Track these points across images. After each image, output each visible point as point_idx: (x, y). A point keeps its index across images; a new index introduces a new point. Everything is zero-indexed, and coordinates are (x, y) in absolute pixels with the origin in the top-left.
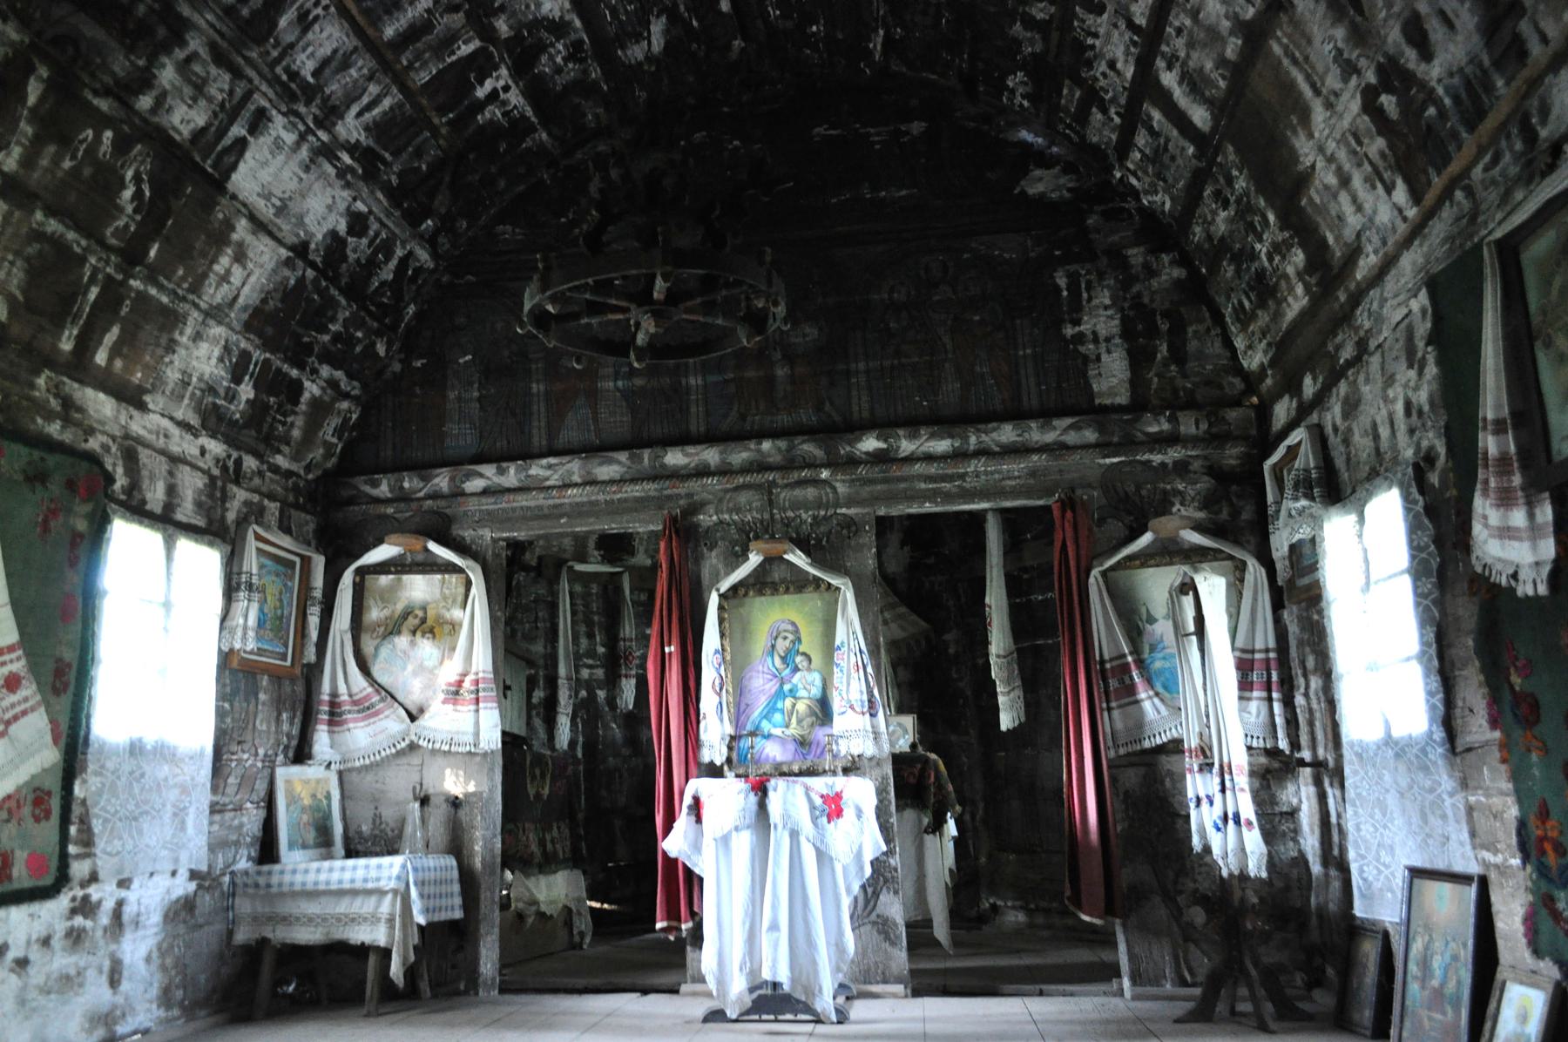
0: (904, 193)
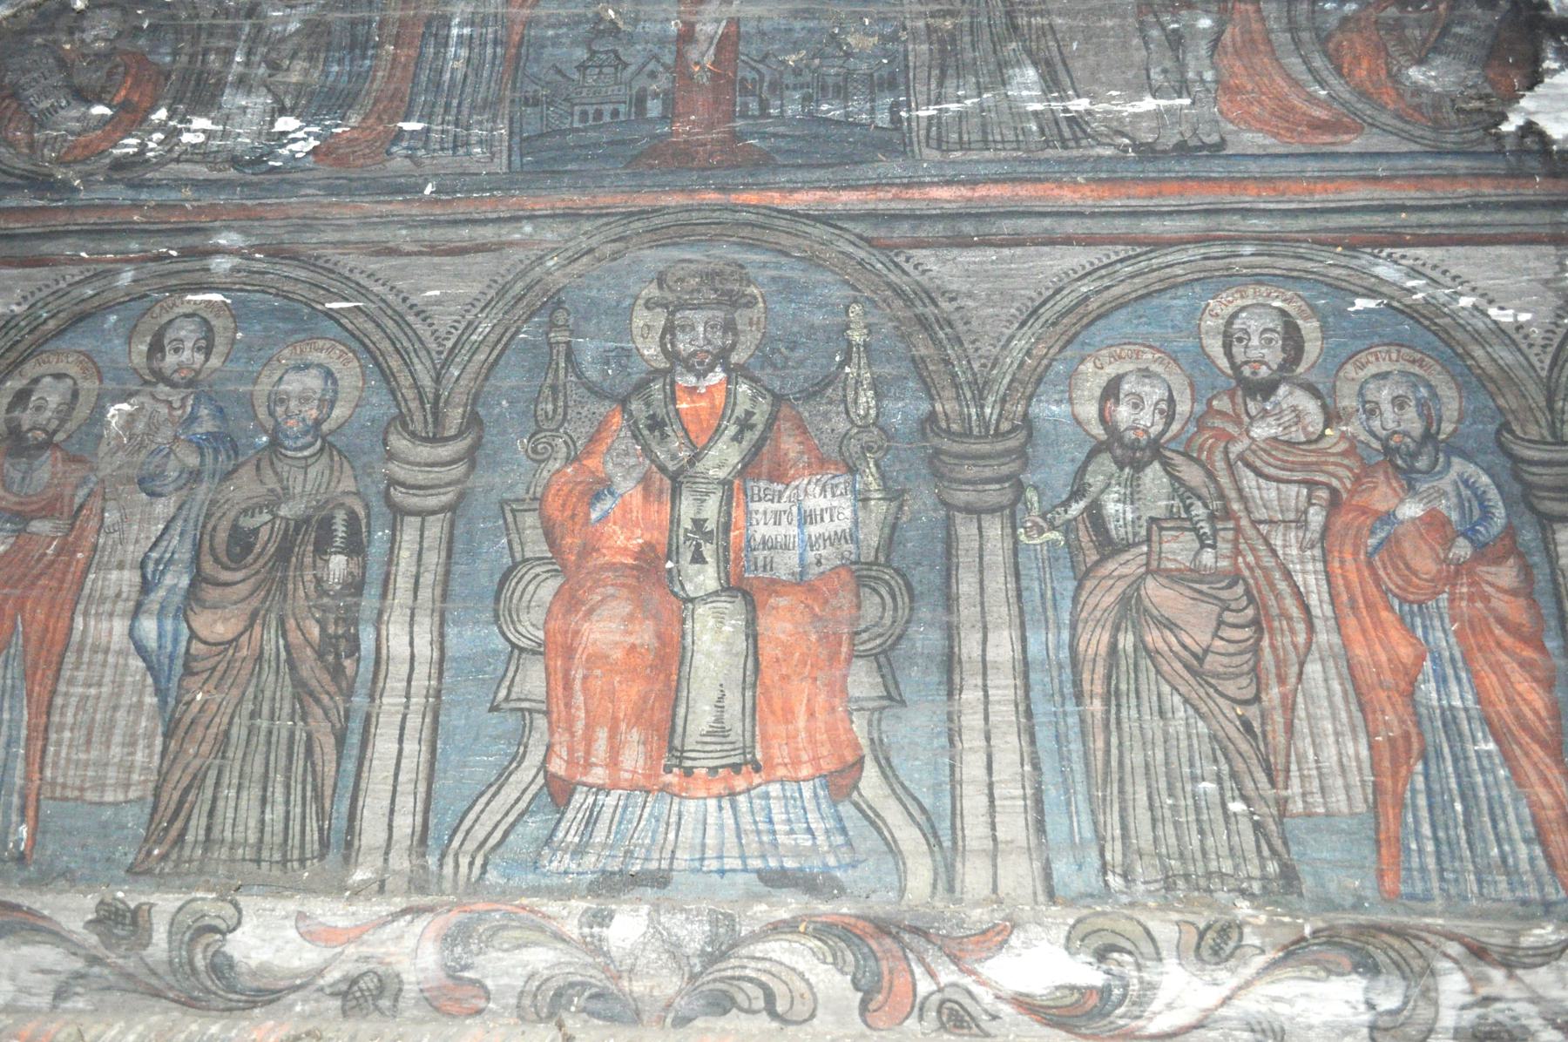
0: (1148, 104)
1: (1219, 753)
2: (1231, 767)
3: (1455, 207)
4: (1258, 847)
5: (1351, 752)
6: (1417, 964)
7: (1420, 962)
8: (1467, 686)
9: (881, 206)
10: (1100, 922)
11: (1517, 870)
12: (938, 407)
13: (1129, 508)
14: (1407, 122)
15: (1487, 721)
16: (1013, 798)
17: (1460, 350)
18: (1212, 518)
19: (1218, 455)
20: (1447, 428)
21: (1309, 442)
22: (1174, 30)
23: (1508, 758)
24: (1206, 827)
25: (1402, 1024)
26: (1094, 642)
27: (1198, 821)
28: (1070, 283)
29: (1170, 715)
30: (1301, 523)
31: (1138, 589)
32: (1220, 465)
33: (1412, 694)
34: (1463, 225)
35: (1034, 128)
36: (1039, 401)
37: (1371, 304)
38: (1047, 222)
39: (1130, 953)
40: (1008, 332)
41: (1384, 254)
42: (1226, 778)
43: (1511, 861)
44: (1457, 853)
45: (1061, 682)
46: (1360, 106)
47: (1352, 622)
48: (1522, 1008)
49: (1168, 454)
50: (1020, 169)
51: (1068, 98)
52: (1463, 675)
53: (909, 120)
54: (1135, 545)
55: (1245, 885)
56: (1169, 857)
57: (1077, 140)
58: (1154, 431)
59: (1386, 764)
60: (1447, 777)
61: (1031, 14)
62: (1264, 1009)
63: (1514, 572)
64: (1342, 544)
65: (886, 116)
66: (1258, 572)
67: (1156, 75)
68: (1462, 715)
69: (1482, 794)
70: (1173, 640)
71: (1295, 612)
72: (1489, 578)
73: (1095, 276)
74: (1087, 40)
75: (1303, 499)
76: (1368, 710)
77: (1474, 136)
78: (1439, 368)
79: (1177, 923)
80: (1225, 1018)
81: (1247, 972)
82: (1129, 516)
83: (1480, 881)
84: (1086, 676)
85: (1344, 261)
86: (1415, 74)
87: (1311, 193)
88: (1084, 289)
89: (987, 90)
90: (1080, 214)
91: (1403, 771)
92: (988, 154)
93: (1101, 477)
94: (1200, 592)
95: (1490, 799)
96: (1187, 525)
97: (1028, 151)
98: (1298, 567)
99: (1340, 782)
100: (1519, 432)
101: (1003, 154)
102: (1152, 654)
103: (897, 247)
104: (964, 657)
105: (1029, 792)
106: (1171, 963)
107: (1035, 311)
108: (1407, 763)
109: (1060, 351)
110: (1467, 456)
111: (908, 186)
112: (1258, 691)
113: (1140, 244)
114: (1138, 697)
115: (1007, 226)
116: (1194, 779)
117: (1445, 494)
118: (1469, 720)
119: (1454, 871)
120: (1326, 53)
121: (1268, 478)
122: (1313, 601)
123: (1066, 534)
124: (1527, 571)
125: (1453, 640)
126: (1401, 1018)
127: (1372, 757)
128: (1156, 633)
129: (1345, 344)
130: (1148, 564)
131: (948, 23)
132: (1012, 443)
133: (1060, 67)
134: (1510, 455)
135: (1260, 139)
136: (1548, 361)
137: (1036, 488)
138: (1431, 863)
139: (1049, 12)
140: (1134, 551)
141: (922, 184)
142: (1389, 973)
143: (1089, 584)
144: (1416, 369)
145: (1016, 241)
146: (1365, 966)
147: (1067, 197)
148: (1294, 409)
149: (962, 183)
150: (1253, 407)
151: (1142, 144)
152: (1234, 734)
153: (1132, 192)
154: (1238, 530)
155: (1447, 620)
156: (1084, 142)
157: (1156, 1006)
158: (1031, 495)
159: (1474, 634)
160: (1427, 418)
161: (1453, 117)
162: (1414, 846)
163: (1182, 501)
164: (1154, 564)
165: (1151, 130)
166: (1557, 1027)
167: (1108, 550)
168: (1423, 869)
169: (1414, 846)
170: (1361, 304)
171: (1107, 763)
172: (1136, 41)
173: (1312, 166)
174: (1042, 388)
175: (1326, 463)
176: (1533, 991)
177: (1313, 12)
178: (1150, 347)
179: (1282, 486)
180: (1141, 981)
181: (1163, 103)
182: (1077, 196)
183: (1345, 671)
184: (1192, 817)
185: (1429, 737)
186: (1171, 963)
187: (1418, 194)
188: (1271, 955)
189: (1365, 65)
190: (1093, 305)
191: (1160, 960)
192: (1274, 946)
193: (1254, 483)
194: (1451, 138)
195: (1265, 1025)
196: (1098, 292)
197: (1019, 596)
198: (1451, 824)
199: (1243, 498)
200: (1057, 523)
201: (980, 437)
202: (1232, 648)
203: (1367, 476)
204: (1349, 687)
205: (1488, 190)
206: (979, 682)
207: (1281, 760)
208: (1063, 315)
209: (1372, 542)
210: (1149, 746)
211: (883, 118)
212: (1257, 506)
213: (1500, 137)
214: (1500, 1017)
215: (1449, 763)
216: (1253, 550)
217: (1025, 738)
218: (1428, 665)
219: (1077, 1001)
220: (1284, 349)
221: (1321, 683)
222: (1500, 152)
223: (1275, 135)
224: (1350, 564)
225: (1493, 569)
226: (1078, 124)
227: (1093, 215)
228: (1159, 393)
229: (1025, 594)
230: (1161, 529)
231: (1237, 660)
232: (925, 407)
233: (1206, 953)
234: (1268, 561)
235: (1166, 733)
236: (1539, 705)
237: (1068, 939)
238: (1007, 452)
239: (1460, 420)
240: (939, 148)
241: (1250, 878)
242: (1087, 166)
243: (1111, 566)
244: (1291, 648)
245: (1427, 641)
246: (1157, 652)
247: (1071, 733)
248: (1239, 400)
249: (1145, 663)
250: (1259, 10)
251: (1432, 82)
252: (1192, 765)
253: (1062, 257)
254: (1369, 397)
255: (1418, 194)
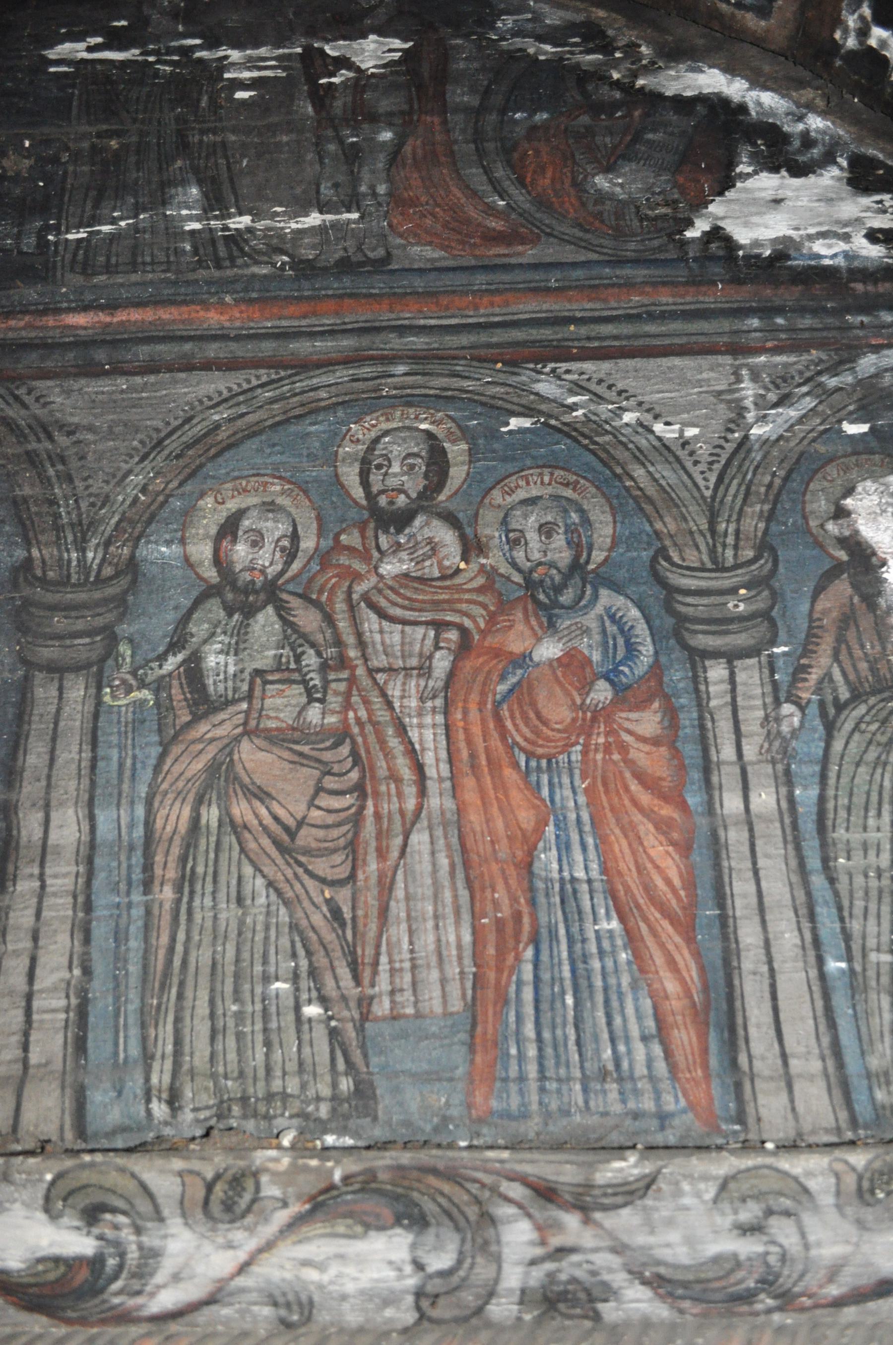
0: (314, 219)
1: (299, 945)
2: (311, 964)
3: (630, 318)
4: (333, 1060)
5: (452, 938)
6: (472, 1212)
7: (476, 1208)
8: (592, 854)
9: (10, 335)
10: (86, 1177)
11: (632, 1078)
12: (35, 553)
13: (231, 660)
14: (587, 231)
15: (612, 893)
16: (54, 1011)
17: (619, 471)
18: (324, 668)
19: (340, 596)
20: (598, 556)
21: (443, 578)
22: (353, 143)
23: (632, 938)
24: (274, 1038)
25: (457, 1288)
26: (173, 818)
27: (265, 1030)
28: (202, 412)
29: (248, 902)
30: (424, 670)
31: (231, 754)
32: (340, 606)
33: (530, 865)
34: (635, 336)
35: (188, 248)
36: (148, 542)
37: (526, 423)
38: (188, 347)
39: (124, 1213)
40: (125, 467)
41: (547, 370)
42: (304, 975)
43: (625, 1065)
44: (563, 1058)
45: (129, 867)
46: (538, 215)
47: (469, 782)
48: (603, 1259)
49: (284, 596)
50: (166, 292)
51: (230, 216)
52: (590, 841)
53: (56, 244)
54: (235, 701)
55: (311, 1108)
56: (226, 1077)
57: (232, 259)
58: (271, 571)
59: (491, 951)
60: (560, 964)
61: (203, 132)
62: (288, 1275)
63: (658, 717)
64: (468, 693)
65: (33, 240)
66: (369, 728)
67: (326, 191)
68: (585, 887)
69: (598, 983)
70: (263, 811)
71: (407, 774)
72: (627, 725)
73: (231, 403)
74: (259, 156)
75: (429, 642)
76: (477, 885)
77: (656, 243)
78: (593, 490)
79: (180, 1174)
80: (243, 1290)
81: (269, 1230)
82: (231, 669)
83: (585, 1090)
84: (159, 858)
85: (501, 378)
86: (601, 182)
87: (476, 307)
88: (216, 417)
89: (145, 210)
90: (224, 338)
91: (510, 959)
92: (135, 278)
93: (206, 626)
94: (301, 754)
95: (606, 989)
96: (296, 676)
97: (178, 272)
98: (415, 721)
99: (435, 975)
100: (676, 559)
101: (150, 276)
102: (237, 829)
103: (20, 379)
104: (24, 840)
105: (74, 1001)
106: (175, 1224)
107: (160, 442)
108: (516, 948)
109: (181, 485)
110: (617, 588)
111: (44, 312)
112: (354, 868)
113: (285, 368)
114: (215, 881)
115: (144, 351)
116: (266, 979)
117: (587, 631)
118: (591, 892)
119: (559, 1080)
120: (509, 164)
121: (393, 620)
122: (429, 758)
123: (157, 692)
124: (671, 714)
125: (582, 799)
126: (455, 1280)
127: (475, 943)
128: (244, 804)
129: (494, 467)
130: (245, 724)
131: (114, 144)
132: (110, 591)
133: (226, 188)
134: (662, 582)
135: (430, 253)
136: (713, 479)
137: (131, 641)
138: (532, 1070)
139: (223, 130)
140: (231, 709)
141: (57, 311)
142: (439, 1224)
143: (176, 750)
144: (568, 493)
145: (151, 368)
146: (410, 1217)
147: (213, 319)
148: (430, 541)
149: (101, 308)
150: (384, 541)
151: (301, 261)
152: (317, 919)
153: (286, 312)
154: (352, 681)
155: (577, 777)
156: (240, 261)
157: (159, 1278)
158: (125, 649)
159: (607, 792)
160: (575, 545)
161: (636, 223)
162: (513, 1051)
163: (293, 649)
164: (253, 723)
165: (314, 247)
166: (645, 1282)
167: (202, 708)
168: (522, 1078)
169: (513, 1051)
170: (515, 423)
171: (169, 962)
172: (310, 156)
173: (480, 280)
174: (153, 526)
175: (460, 601)
176: (616, 1239)
177: (502, 122)
178: (280, 478)
179: (408, 629)
180: (141, 1247)
181: (329, 217)
182: (227, 317)
183: (455, 840)
184: (259, 1026)
185: (543, 919)
186: (175, 1224)
187: (589, 306)
188: (296, 1208)
189: (549, 174)
190: (222, 435)
191: (161, 1219)
192: (299, 1197)
193: (376, 627)
194: (632, 246)
195: (291, 1297)
196: (230, 420)
197: (93, 767)
198: (559, 1020)
199: (362, 644)
200: (149, 679)
201: (79, 585)
202: (330, 819)
203: (502, 614)
204: (458, 860)
205: (666, 299)
206: (36, 871)
207: (370, 951)
208: (189, 446)
209: (502, 688)
210: (220, 942)
211: (29, 243)
212: (376, 652)
213: (684, 244)
214: (579, 1274)
215: (564, 946)
216: (366, 702)
217: (79, 936)
218: (550, 830)
219: (64, 1275)
220: (426, 476)
221: (427, 857)
222: (683, 259)
223: (443, 248)
224: (474, 714)
225: (633, 715)
226: (237, 244)
227: (238, 338)
228: (283, 528)
229: (101, 764)
230: (266, 683)
231: (335, 833)
232: (20, 554)
233: (216, 1208)
234: (383, 715)
235: (242, 923)
236: (674, 875)
237: (47, 1198)
238: (106, 601)
239: (614, 545)
240: (84, 272)
241: (318, 1099)
242: (239, 286)
243: (203, 728)
244: (397, 818)
245: (552, 801)
246: (245, 827)
247: (132, 929)
248: (370, 533)
249: (229, 839)
250: (445, 122)
251: (618, 189)
252: (265, 962)
253: (198, 384)
254: (514, 525)
255: (589, 306)
